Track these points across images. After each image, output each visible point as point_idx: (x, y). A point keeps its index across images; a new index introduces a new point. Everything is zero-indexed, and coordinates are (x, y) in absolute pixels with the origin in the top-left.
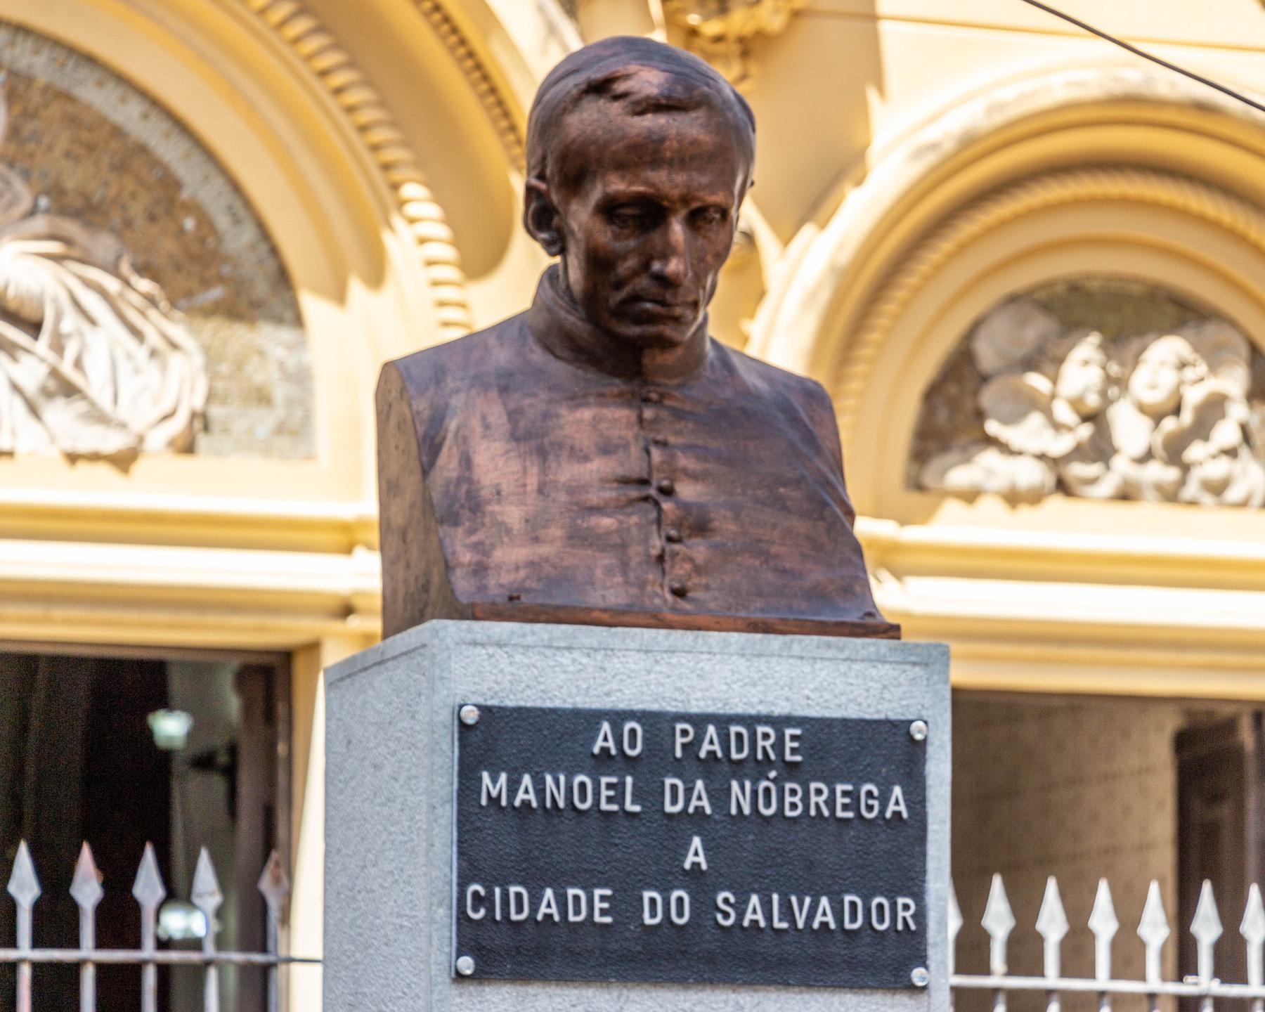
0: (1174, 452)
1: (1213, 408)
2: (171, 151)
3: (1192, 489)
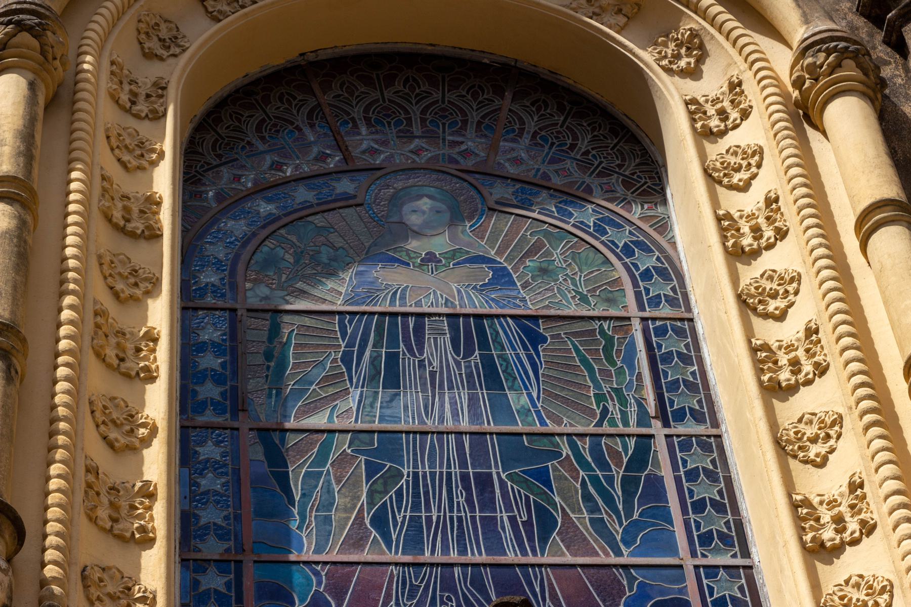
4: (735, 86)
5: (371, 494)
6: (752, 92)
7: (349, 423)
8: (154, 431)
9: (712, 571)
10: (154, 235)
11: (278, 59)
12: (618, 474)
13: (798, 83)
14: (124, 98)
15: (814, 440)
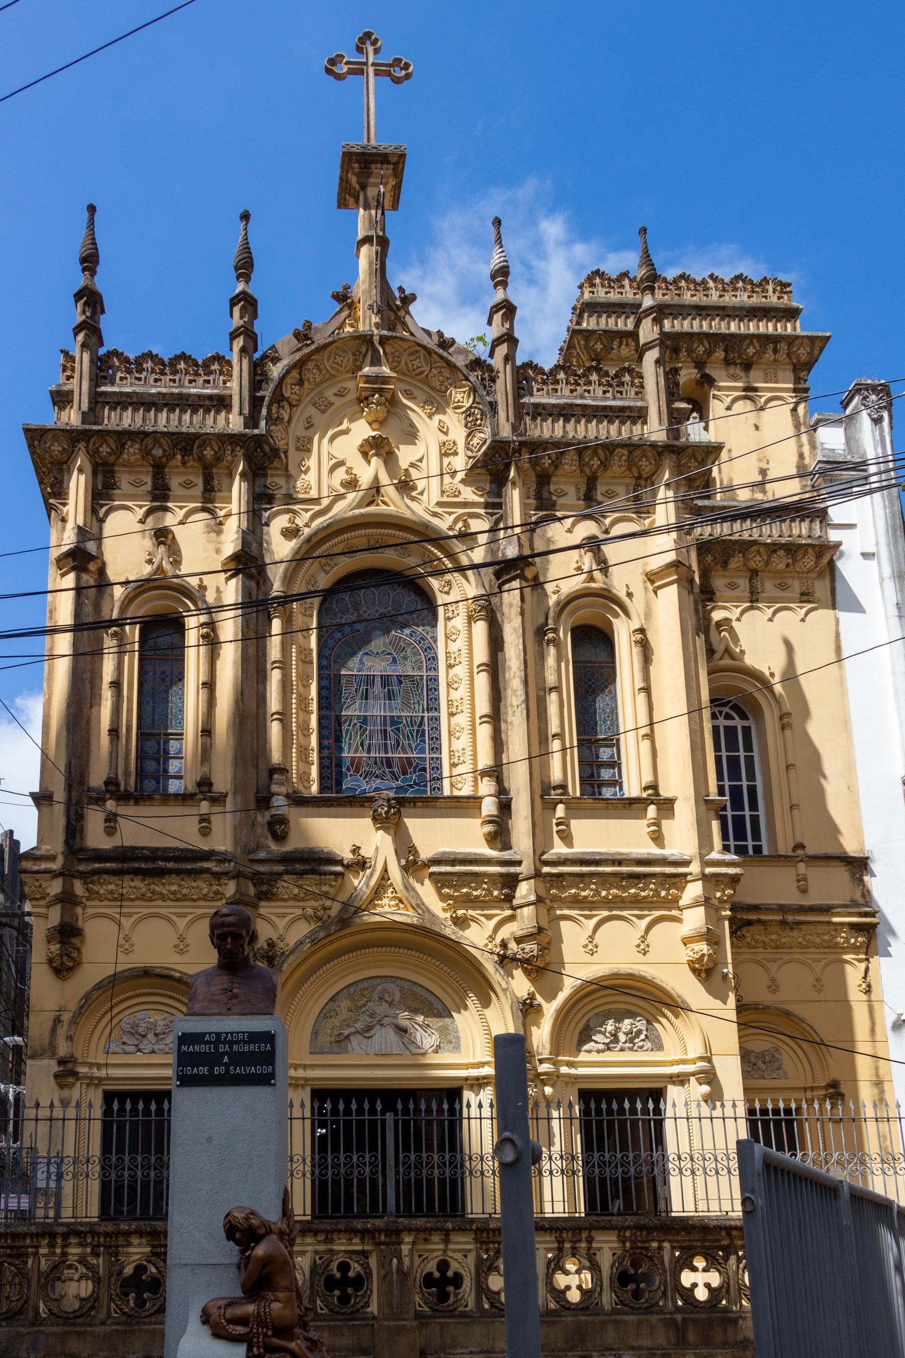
0: (631, 1041)
1: (639, 1032)
2: (431, 999)
3: (635, 1048)
7: (357, 713)
9: (433, 758)
12: (416, 728)
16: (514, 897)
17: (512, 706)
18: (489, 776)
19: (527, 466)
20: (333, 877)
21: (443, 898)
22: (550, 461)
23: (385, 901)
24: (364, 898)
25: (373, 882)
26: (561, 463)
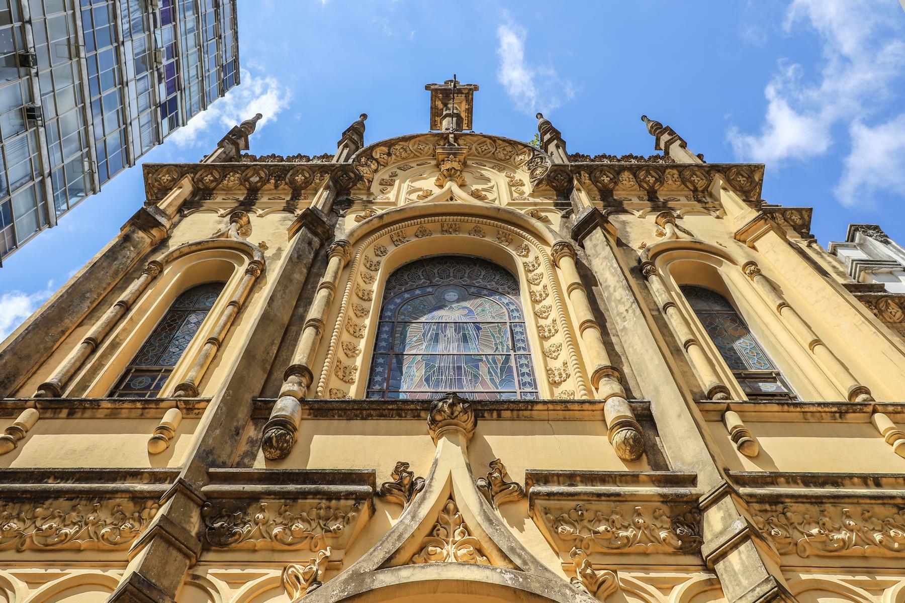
4: (537, 258)
5: (426, 372)
6: (541, 259)
8: (360, 352)
10: (370, 300)
11: (415, 258)
13: (552, 255)
14: (368, 265)
15: (554, 352)
16: (701, 543)
17: (619, 314)
18: (608, 376)
19: (587, 181)
20: (351, 502)
21: (560, 545)
22: (608, 179)
23: (450, 549)
24: (406, 536)
25: (424, 511)
26: (619, 179)
